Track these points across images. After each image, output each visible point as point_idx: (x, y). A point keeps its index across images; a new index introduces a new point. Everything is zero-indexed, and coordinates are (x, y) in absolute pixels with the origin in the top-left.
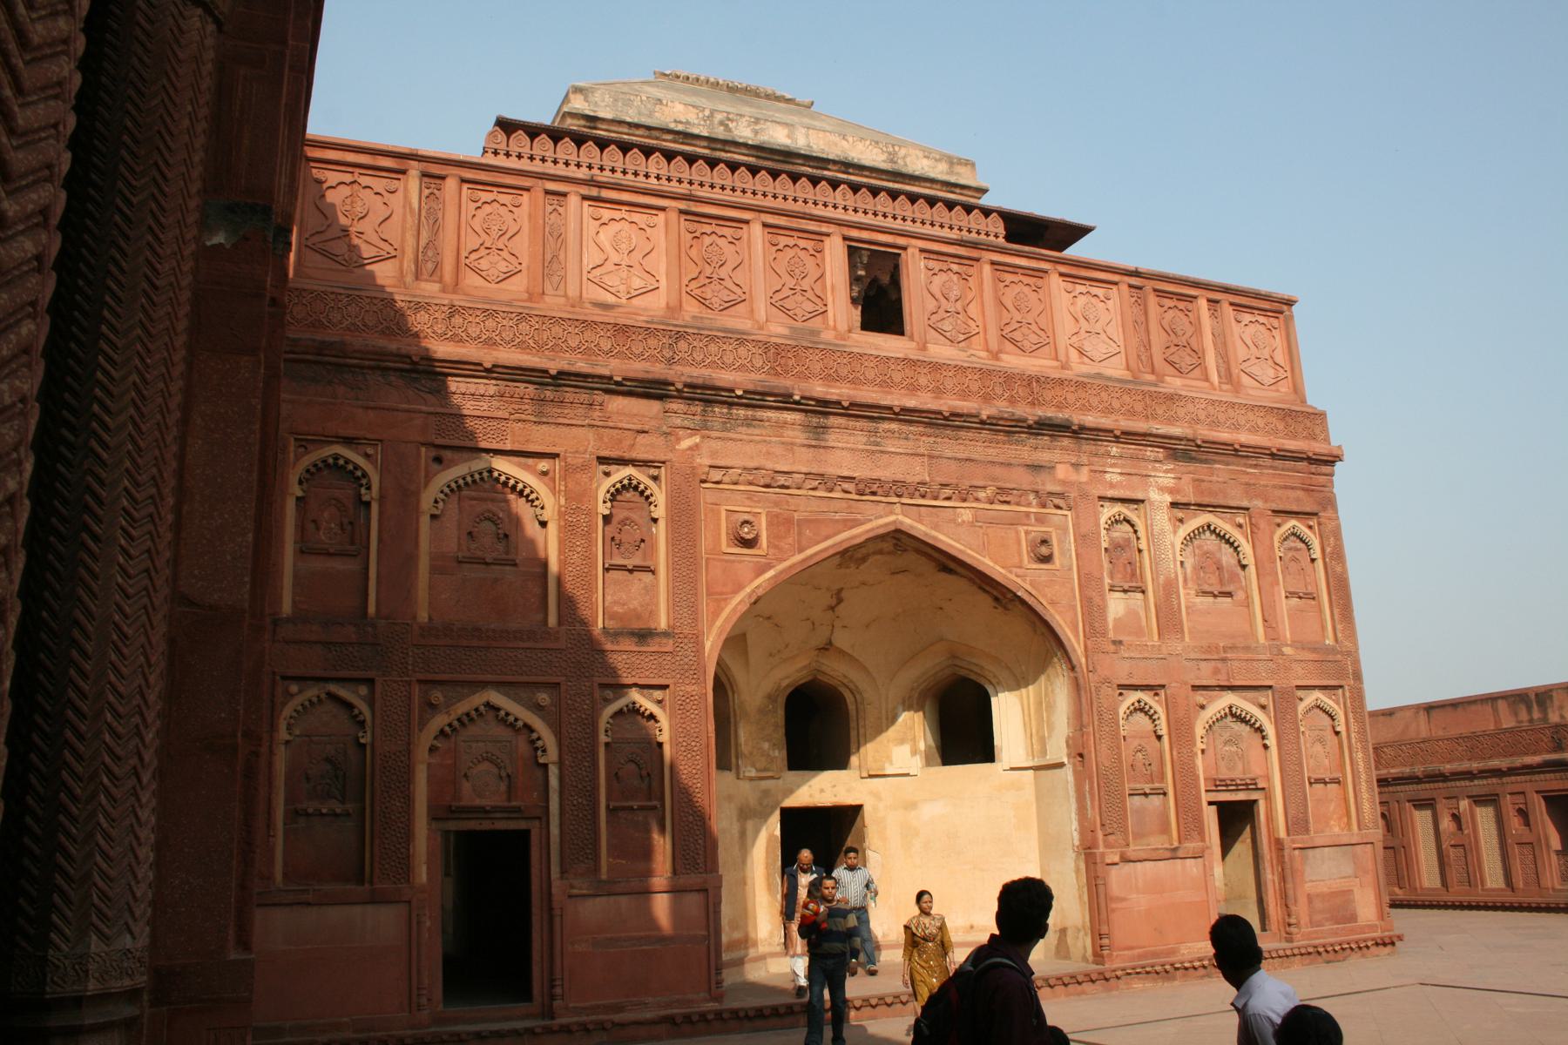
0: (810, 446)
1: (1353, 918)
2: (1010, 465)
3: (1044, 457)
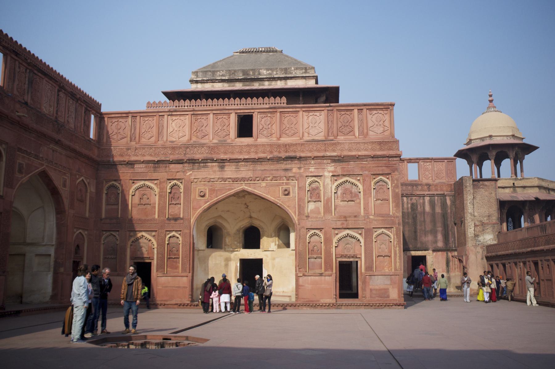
1: (388, 297)
2: (278, 170)
3: (288, 166)
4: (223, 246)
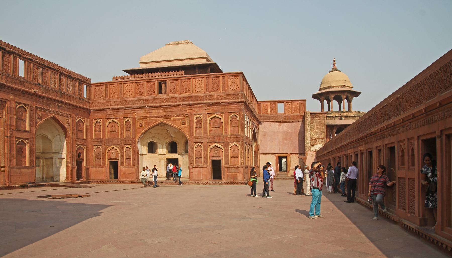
3: (185, 109)
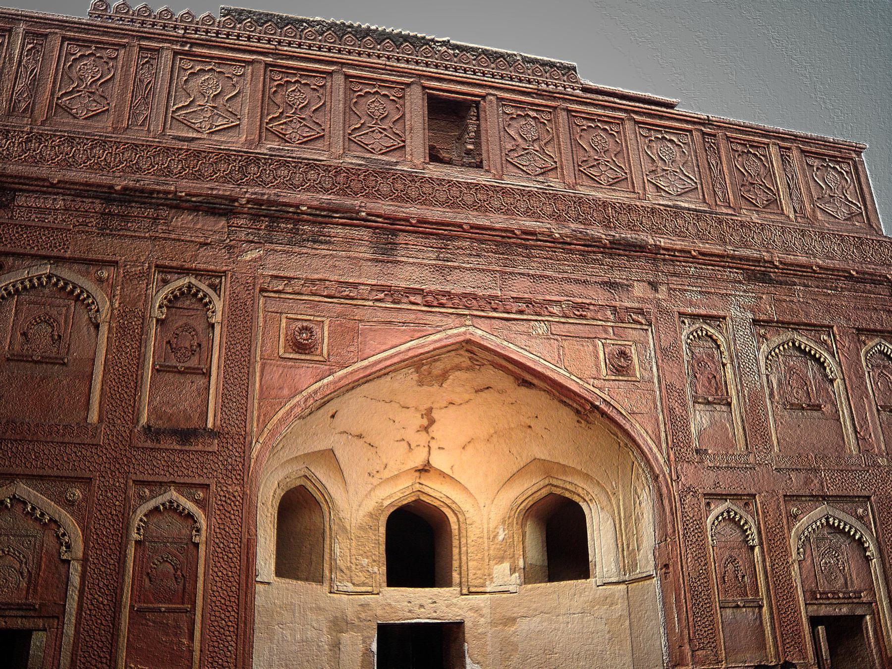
0: (377, 261)
4: (327, 572)
